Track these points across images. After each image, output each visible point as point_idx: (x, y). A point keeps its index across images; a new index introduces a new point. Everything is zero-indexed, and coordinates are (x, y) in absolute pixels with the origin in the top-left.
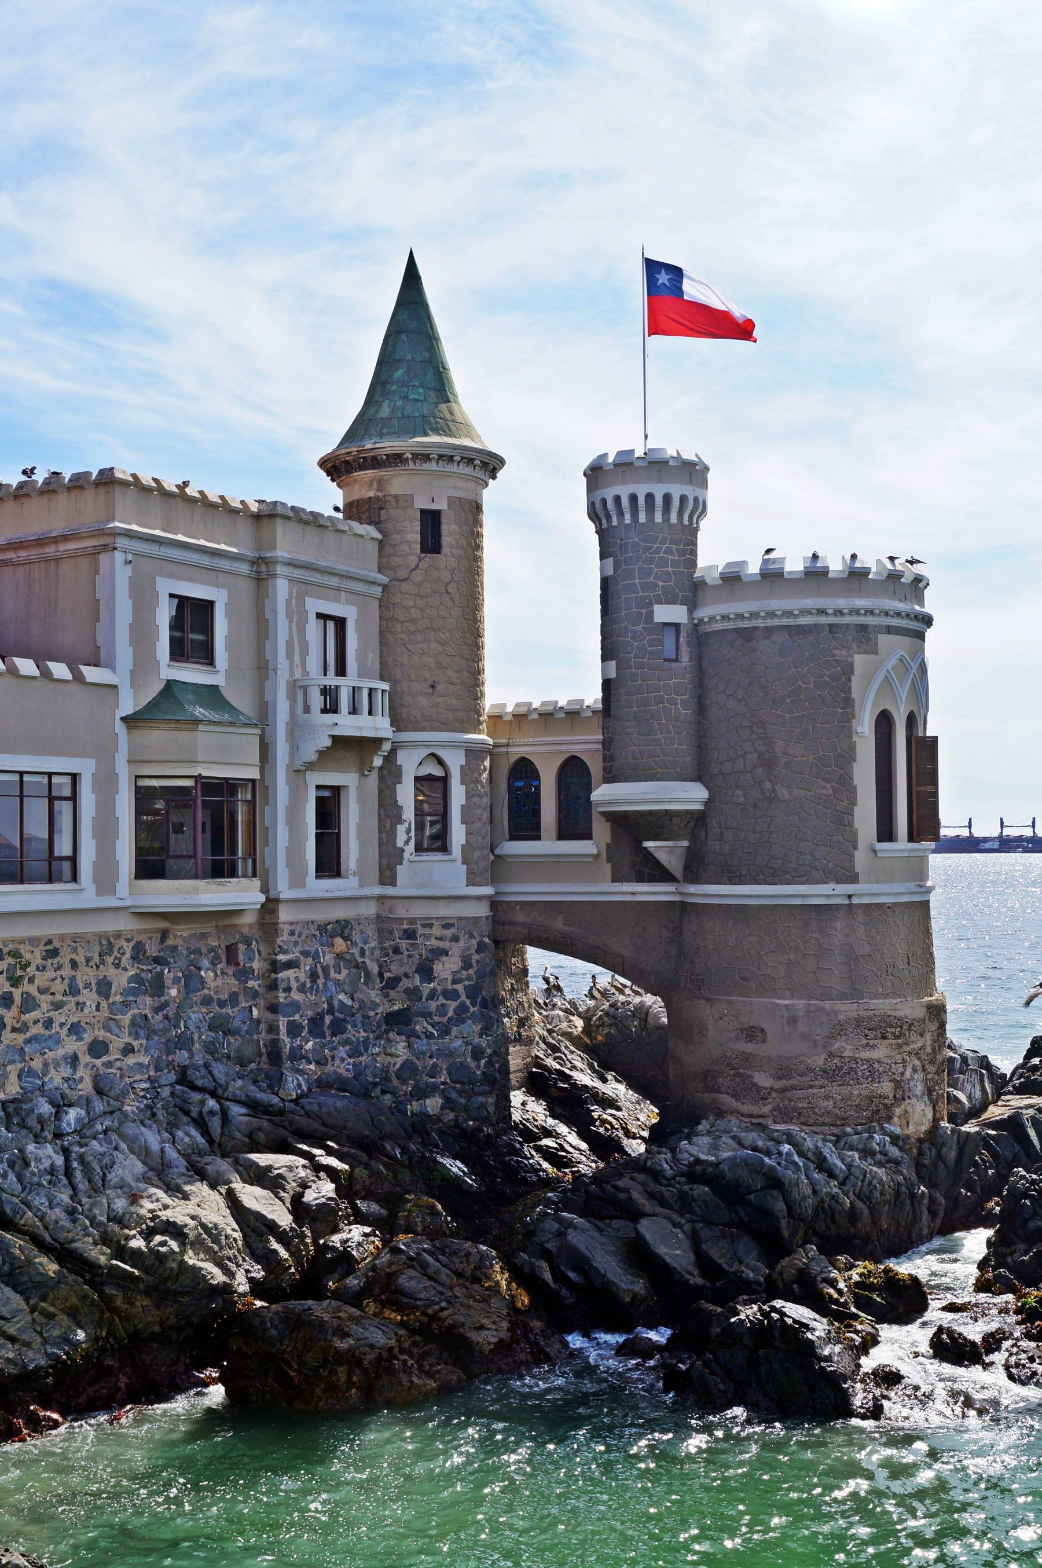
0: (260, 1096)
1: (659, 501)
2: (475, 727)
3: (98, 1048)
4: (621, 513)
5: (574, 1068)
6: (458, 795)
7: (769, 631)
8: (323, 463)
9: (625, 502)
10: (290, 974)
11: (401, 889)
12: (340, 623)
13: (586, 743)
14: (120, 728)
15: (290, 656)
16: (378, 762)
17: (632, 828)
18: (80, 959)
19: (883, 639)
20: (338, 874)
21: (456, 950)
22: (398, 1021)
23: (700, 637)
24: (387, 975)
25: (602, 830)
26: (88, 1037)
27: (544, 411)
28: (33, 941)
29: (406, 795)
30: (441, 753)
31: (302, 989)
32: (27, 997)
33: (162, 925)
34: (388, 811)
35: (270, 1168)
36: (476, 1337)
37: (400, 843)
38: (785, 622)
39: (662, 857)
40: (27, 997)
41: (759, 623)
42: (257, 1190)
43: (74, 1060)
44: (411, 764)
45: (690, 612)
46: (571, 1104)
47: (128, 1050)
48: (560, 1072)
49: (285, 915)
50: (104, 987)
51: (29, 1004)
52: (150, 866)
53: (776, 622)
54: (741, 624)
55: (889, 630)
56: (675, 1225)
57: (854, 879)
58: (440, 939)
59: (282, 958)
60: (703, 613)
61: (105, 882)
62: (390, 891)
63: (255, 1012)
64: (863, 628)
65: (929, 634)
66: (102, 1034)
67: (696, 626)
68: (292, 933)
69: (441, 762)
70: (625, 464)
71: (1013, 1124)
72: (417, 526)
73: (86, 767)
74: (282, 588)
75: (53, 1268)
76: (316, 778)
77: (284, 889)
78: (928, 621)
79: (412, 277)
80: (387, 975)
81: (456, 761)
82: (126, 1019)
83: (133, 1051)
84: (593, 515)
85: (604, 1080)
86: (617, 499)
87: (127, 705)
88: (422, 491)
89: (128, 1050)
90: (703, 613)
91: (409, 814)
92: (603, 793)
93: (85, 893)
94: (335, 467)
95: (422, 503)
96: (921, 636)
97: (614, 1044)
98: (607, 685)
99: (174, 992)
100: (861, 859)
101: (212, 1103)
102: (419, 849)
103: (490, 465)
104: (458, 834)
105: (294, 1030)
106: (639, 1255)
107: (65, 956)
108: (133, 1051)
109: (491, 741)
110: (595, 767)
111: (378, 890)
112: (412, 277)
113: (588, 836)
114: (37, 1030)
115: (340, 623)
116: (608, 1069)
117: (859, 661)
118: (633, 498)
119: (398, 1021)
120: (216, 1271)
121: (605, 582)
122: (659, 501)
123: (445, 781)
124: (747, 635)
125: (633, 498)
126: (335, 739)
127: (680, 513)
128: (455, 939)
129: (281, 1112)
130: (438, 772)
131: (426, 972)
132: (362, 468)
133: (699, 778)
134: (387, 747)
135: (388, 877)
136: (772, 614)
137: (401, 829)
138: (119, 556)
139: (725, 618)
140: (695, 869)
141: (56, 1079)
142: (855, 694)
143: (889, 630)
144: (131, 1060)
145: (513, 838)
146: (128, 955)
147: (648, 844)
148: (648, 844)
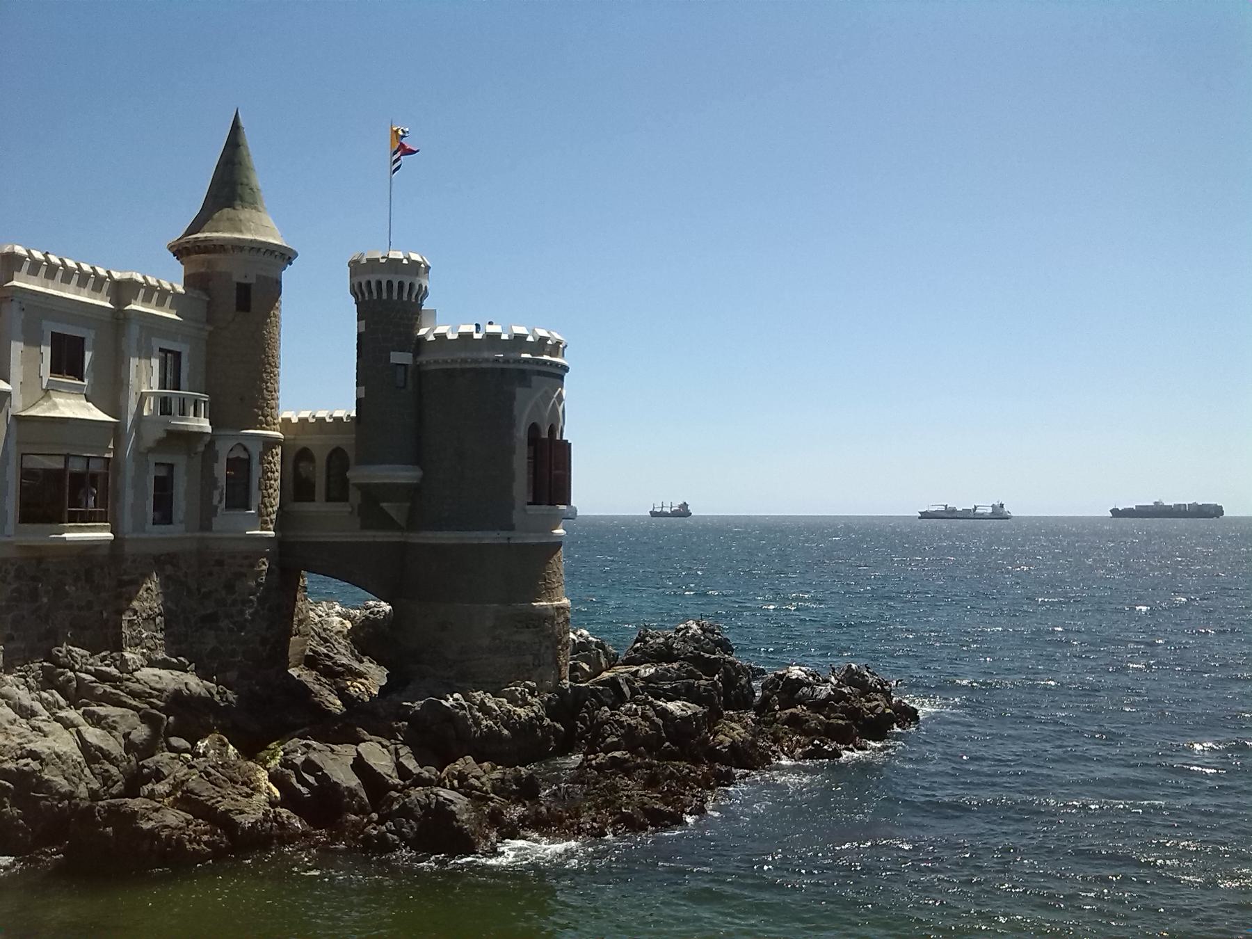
0: (104, 668)
1: (396, 285)
2: (268, 425)
4: (370, 292)
5: (339, 652)
7: (463, 371)
8: (171, 248)
9: (373, 285)
12: (178, 355)
13: (346, 441)
15: (138, 375)
16: (201, 448)
17: (372, 496)
19: (535, 379)
20: (170, 523)
23: (419, 373)
24: (203, 590)
25: (355, 497)
29: (221, 470)
30: (246, 443)
34: (208, 481)
35: (106, 717)
36: (238, 818)
37: (215, 502)
38: (473, 366)
39: (393, 513)
41: (458, 366)
42: (98, 731)
44: (224, 449)
45: (415, 357)
46: (334, 674)
48: (327, 655)
53: (468, 366)
54: (445, 366)
55: (539, 373)
56: (383, 746)
57: (511, 528)
58: (241, 566)
59: (125, 578)
60: (423, 359)
62: (207, 534)
63: (105, 615)
64: (523, 372)
65: (567, 376)
67: (418, 366)
68: (134, 561)
69: (245, 449)
70: (373, 262)
71: (613, 682)
72: (234, 294)
76: (153, 459)
78: (566, 369)
79: (236, 127)
80: (203, 590)
83: (13, 638)
84: (353, 293)
85: (361, 662)
86: (369, 283)
90: (423, 359)
91: (223, 482)
92: (359, 475)
94: (181, 251)
95: (238, 278)
96: (562, 378)
97: (367, 638)
98: (359, 402)
99: (45, 600)
100: (517, 517)
101: (71, 674)
102: (229, 507)
103: (285, 256)
106: (360, 766)
108: (13, 638)
109: (281, 436)
110: (351, 455)
111: (198, 534)
112: (236, 127)
113: (346, 500)
115: (178, 355)
116: (364, 655)
117: (520, 392)
118: (379, 283)
119: (210, 620)
120: (65, 782)
121: (359, 335)
122: (396, 285)
123: (248, 462)
124: (449, 374)
125: (379, 283)
127: (410, 294)
129: (121, 680)
130: (243, 455)
131: (230, 587)
132: (197, 253)
134: (208, 439)
135: (206, 525)
137: (216, 494)
139: (436, 362)
140: (413, 523)
142: (516, 412)
143: (539, 373)
145: (296, 500)
146: (12, 574)
147: (384, 505)
148: (384, 505)
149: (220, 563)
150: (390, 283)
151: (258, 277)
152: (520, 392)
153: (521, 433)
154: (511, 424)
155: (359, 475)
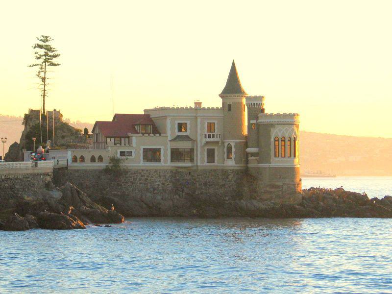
3: (163, 184)
6: (233, 150)
10: (200, 176)
11: (225, 165)
14: (169, 142)
18: (161, 172)
19: (276, 126)
21: (232, 174)
22: (224, 185)
23: (258, 125)
26: (162, 182)
27: (250, 86)
28: (153, 170)
31: (202, 179)
32: (151, 176)
33: (177, 168)
40: (151, 176)
43: (159, 185)
44: (226, 145)
47: (168, 185)
49: (199, 168)
50: (165, 176)
51: (152, 177)
52: (172, 160)
55: (277, 124)
57: (270, 163)
61: (166, 161)
64: (272, 124)
66: (164, 182)
72: (227, 107)
73: (162, 148)
74: (199, 120)
75: (145, 206)
77: (199, 164)
81: (233, 145)
82: (169, 181)
87: (169, 139)
88: (230, 101)
89: (168, 185)
90: (259, 121)
93: (162, 163)
104: (233, 156)
105: (200, 185)
107: (158, 172)
111: (222, 165)
114: (153, 180)
117: (272, 129)
123: (231, 147)
126: (207, 142)
128: (232, 173)
131: (227, 177)
133: (258, 146)
136: (275, 122)
138: (168, 119)
141: (156, 187)
143: (277, 124)
144: (169, 186)
149: (225, 172)
150: (252, 104)
151: (233, 103)
152: (272, 129)
153: (272, 139)
154: (270, 138)
155: (249, 150)
